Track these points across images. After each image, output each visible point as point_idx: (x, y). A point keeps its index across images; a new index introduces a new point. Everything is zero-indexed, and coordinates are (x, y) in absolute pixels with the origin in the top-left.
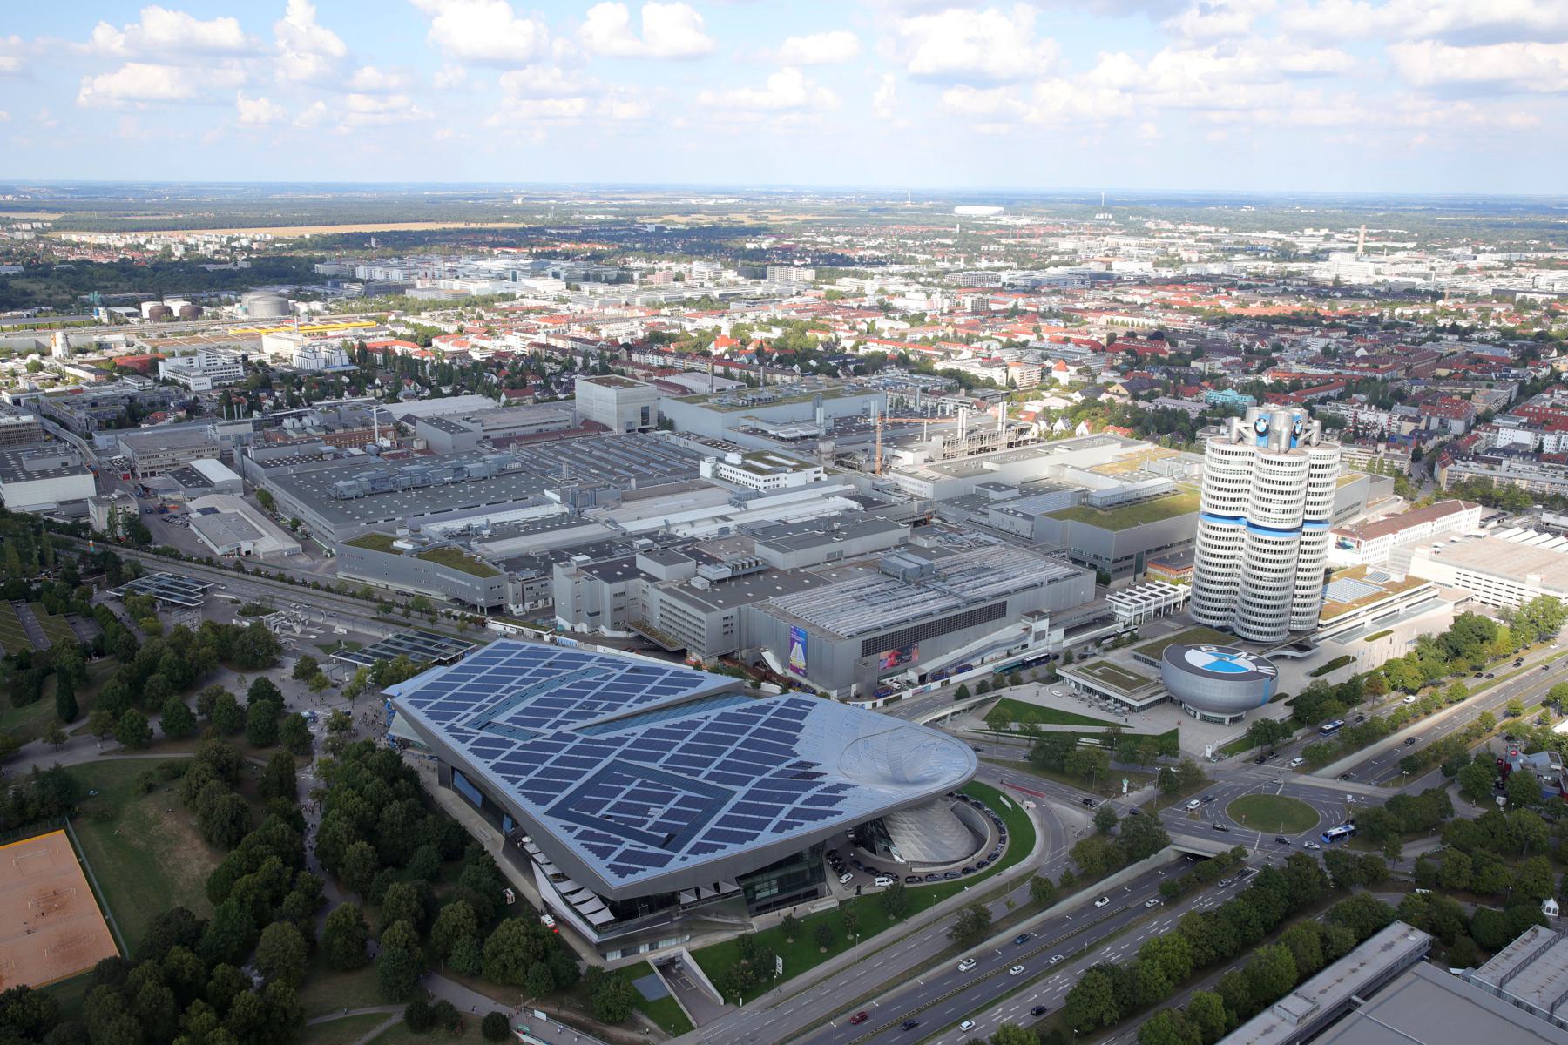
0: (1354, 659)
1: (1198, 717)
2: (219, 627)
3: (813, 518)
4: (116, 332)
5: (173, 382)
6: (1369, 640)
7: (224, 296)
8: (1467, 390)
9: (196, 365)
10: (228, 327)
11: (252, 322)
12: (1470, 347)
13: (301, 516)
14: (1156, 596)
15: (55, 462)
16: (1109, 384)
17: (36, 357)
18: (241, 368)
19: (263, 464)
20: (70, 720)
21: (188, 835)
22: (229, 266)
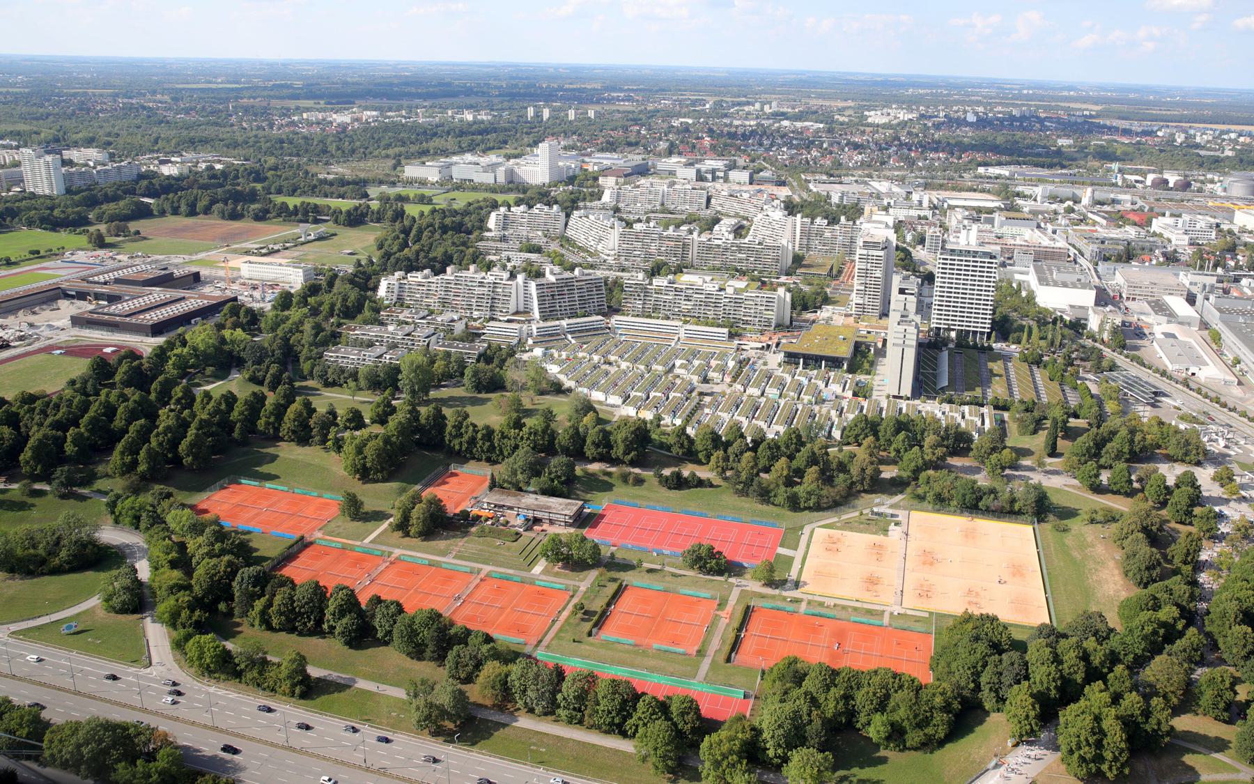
2: (1163, 423)
4: (1126, 193)
5: (1161, 235)
7: (1209, 176)
9: (1180, 225)
10: (1208, 200)
11: (1228, 198)
13: (1242, 357)
15: (1074, 278)
17: (1070, 203)
18: (1214, 233)
19: (1219, 310)
20: (1051, 455)
21: (1111, 564)
22: (1217, 154)
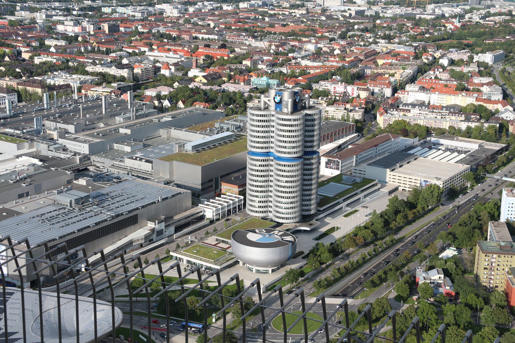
0: (338, 228)
1: (254, 271)
3: (8, 172)
6: (345, 216)
8: (392, 72)
12: (391, 47)
14: (227, 202)
16: (195, 77)
